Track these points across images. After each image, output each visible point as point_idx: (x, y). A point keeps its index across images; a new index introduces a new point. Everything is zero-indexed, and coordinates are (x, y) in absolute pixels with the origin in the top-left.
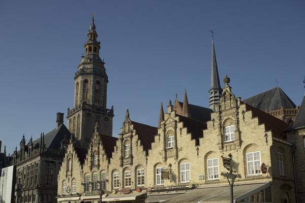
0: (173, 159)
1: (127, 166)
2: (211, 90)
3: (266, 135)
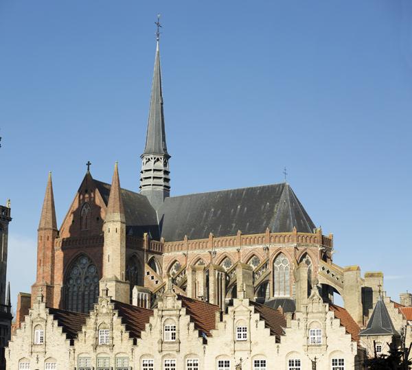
0: (246, 352)
1: (171, 352)
2: (149, 153)
3: (352, 345)
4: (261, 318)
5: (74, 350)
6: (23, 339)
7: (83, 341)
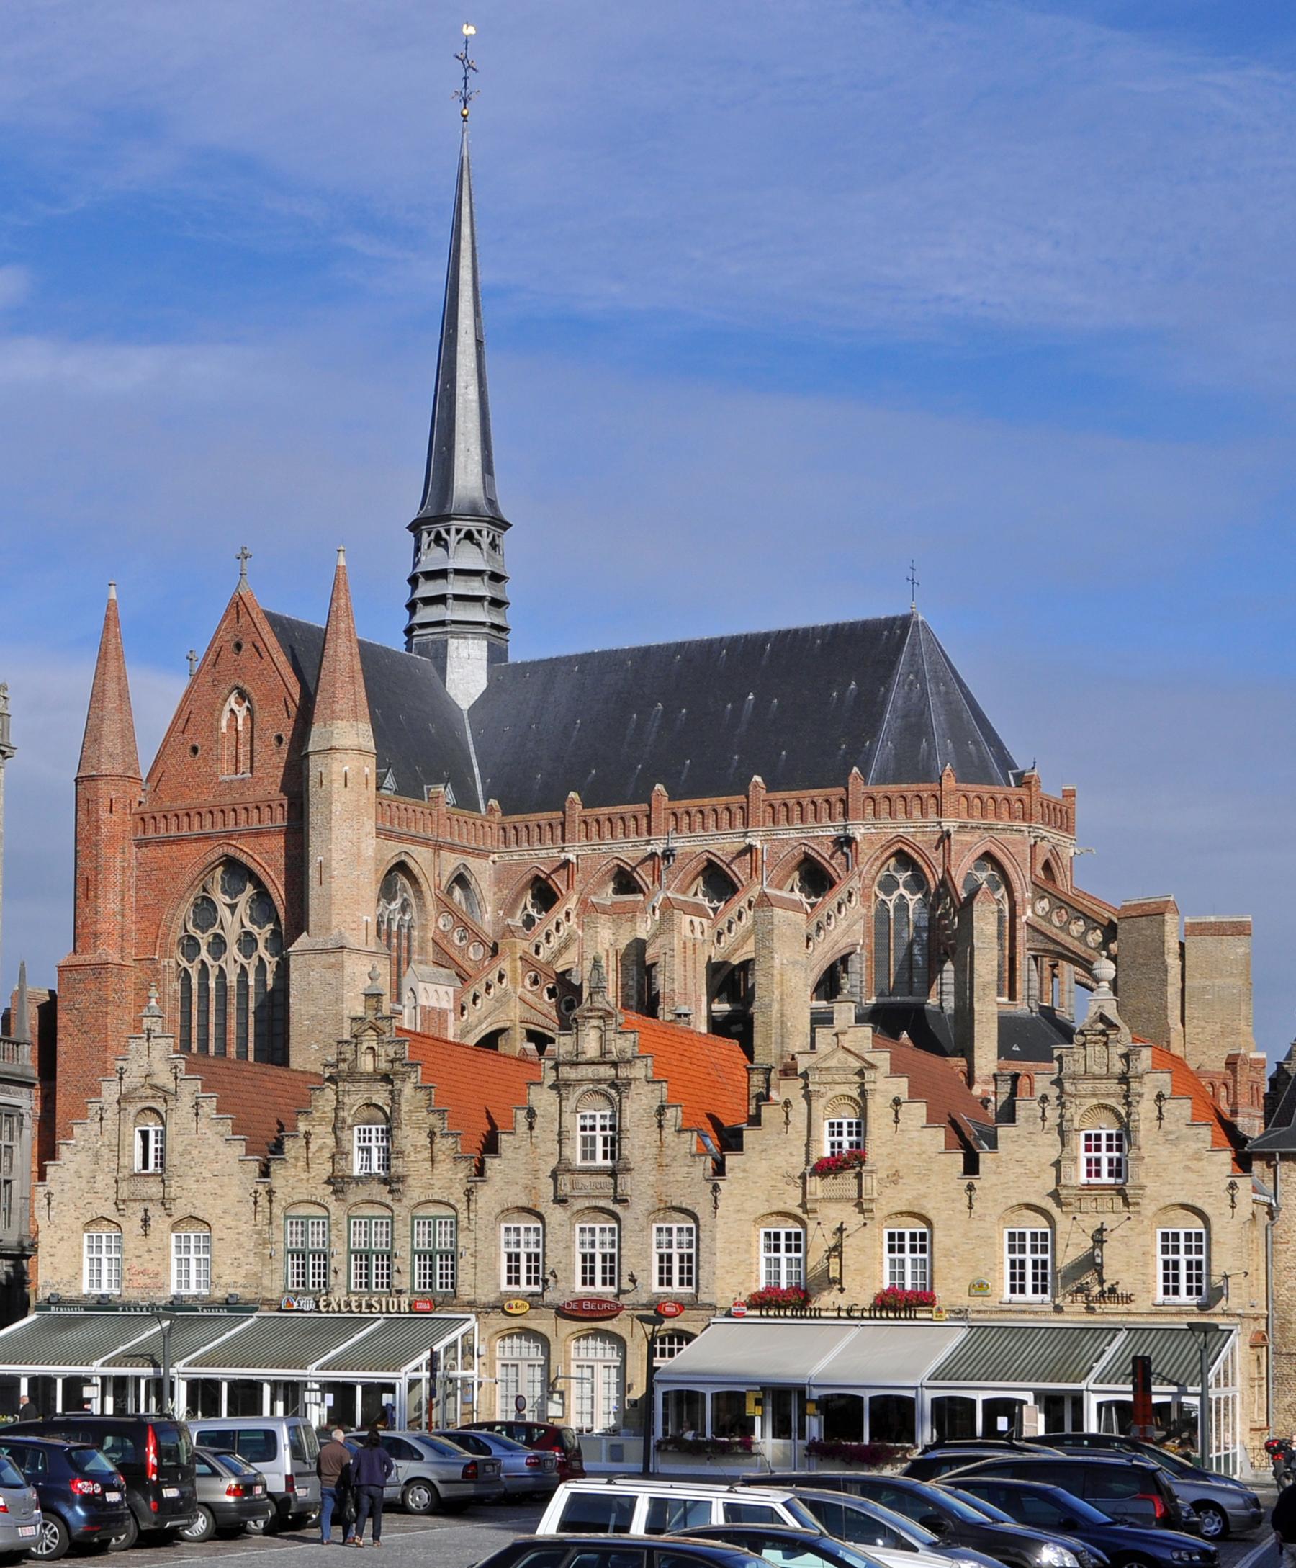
4: (914, 1095)
5: (270, 1192)
6: (97, 1155)
7: (302, 1164)
